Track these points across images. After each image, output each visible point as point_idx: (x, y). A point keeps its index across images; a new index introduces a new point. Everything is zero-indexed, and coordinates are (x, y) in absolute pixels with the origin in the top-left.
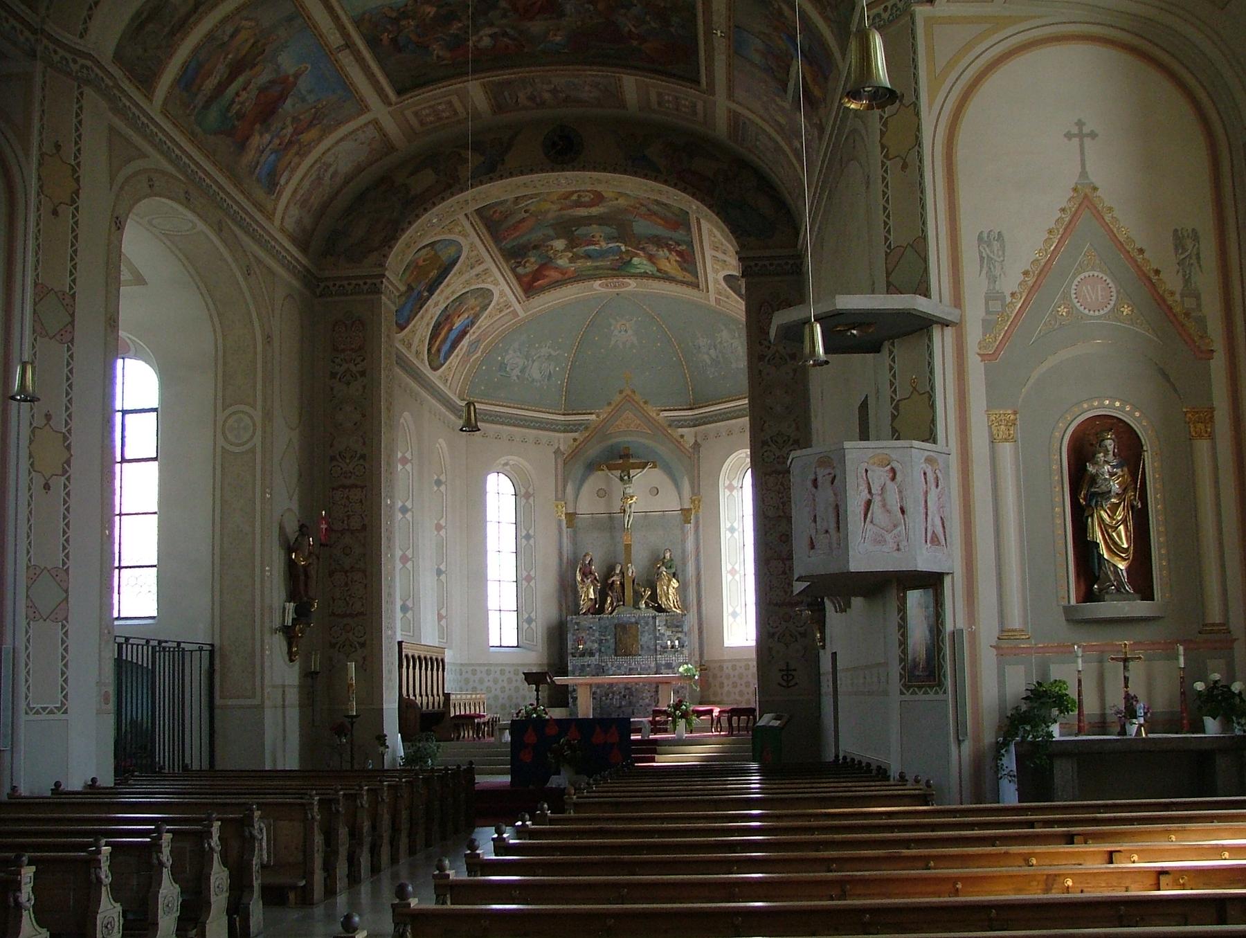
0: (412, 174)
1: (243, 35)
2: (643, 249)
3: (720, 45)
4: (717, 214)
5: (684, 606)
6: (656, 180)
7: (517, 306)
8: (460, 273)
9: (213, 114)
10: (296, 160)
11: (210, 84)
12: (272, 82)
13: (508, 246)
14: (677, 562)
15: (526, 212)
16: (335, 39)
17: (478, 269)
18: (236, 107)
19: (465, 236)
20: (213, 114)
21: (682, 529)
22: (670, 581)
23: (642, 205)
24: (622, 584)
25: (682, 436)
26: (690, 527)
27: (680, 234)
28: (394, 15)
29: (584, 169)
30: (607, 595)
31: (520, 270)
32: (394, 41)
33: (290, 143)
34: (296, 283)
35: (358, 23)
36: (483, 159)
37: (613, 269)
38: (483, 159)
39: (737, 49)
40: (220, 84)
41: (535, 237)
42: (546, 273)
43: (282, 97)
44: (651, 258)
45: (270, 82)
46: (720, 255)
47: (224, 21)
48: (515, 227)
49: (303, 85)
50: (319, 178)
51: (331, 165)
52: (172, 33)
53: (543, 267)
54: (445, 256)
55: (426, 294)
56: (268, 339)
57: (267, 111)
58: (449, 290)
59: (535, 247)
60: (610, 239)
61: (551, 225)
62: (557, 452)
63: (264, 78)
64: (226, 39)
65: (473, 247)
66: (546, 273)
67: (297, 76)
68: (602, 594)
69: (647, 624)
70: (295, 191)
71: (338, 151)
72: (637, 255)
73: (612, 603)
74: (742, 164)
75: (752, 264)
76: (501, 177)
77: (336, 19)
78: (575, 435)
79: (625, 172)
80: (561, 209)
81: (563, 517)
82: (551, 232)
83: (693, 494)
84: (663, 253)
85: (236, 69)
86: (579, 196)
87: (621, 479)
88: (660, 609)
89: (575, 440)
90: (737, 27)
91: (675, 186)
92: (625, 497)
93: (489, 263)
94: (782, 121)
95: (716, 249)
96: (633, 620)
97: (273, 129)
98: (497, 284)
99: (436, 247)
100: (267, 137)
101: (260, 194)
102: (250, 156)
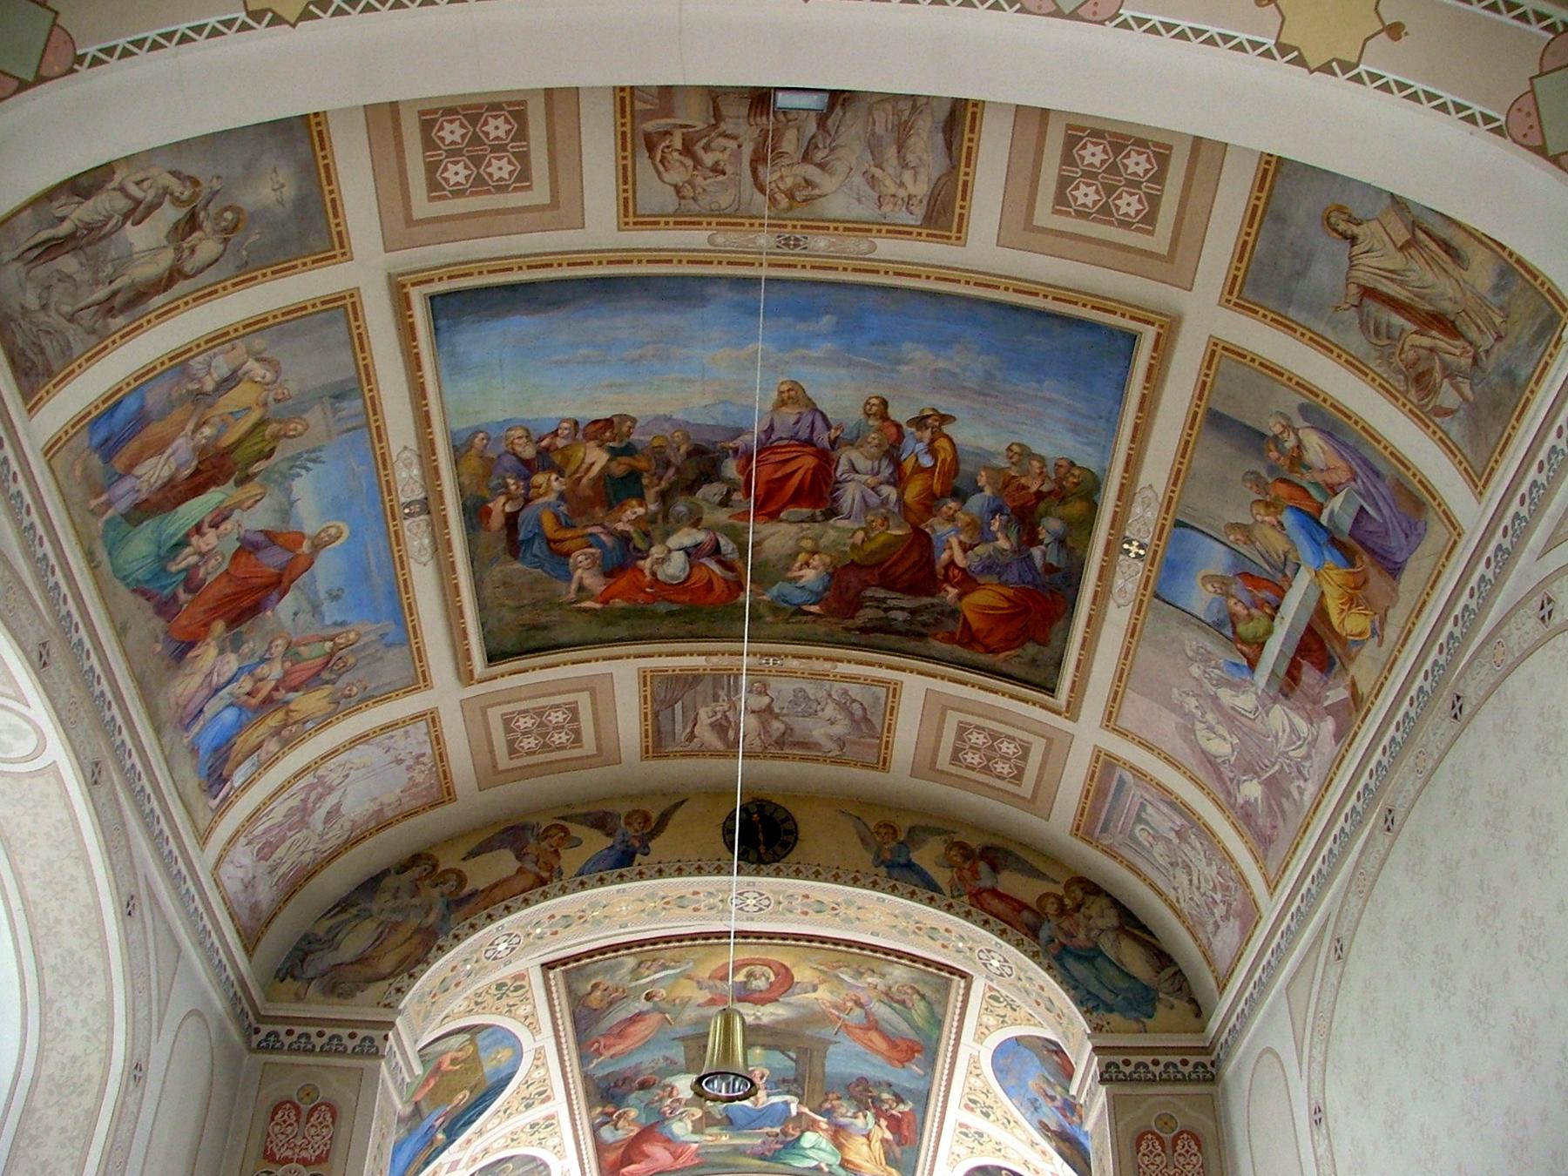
0: (472, 854)
1: (242, 395)
2: (828, 1113)
3: (1129, 578)
4: (1048, 969)
6: (931, 901)
8: (506, 1112)
9: (141, 546)
10: (272, 746)
11: (154, 472)
12: (271, 536)
13: (600, 1073)
15: (649, 997)
16: (407, 481)
17: (538, 1112)
18: (187, 558)
19: (534, 1028)
20: (141, 546)
23: (858, 1003)
27: (904, 1076)
28: (529, 452)
29: (797, 874)
31: (607, 1134)
32: (511, 521)
33: (269, 701)
34: (218, 1003)
35: (459, 452)
36: (609, 842)
37: (762, 1157)
38: (609, 842)
39: (1160, 593)
40: (170, 483)
41: (648, 1060)
42: (647, 1148)
43: (279, 584)
44: (838, 1134)
45: (266, 533)
46: (976, 1121)
47: (219, 339)
48: (621, 1031)
49: (326, 571)
50: (305, 810)
51: (331, 789)
52: (108, 308)
53: (647, 1133)
54: (494, 1060)
55: (440, 1136)
56: (136, 1072)
57: (245, 602)
58: (478, 1145)
59: (644, 1086)
60: (781, 1083)
61: (683, 1039)
63: (257, 519)
64: (209, 386)
65: (539, 1054)
66: (647, 1148)
67: (318, 546)
70: (253, 817)
71: (350, 768)
72: (813, 1126)
74: (1091, 888)
75: (1119, 1059)
76: (641, 876)
77: (423, 420)
79: (874, 885)
82: (678, 1053)
84: (865, 1121)
85: (213, 468)
86: (750, 975)
90: (1179, 524)
91: (967, 915)
93: (559, 1105)
94: (1220, 747)
95: (971, 1104)
97: (245, 649)
98: (561, 1155)
99: (479, 1037)
100: (232, 663)
101: (192, 783)
102: (187, 685)
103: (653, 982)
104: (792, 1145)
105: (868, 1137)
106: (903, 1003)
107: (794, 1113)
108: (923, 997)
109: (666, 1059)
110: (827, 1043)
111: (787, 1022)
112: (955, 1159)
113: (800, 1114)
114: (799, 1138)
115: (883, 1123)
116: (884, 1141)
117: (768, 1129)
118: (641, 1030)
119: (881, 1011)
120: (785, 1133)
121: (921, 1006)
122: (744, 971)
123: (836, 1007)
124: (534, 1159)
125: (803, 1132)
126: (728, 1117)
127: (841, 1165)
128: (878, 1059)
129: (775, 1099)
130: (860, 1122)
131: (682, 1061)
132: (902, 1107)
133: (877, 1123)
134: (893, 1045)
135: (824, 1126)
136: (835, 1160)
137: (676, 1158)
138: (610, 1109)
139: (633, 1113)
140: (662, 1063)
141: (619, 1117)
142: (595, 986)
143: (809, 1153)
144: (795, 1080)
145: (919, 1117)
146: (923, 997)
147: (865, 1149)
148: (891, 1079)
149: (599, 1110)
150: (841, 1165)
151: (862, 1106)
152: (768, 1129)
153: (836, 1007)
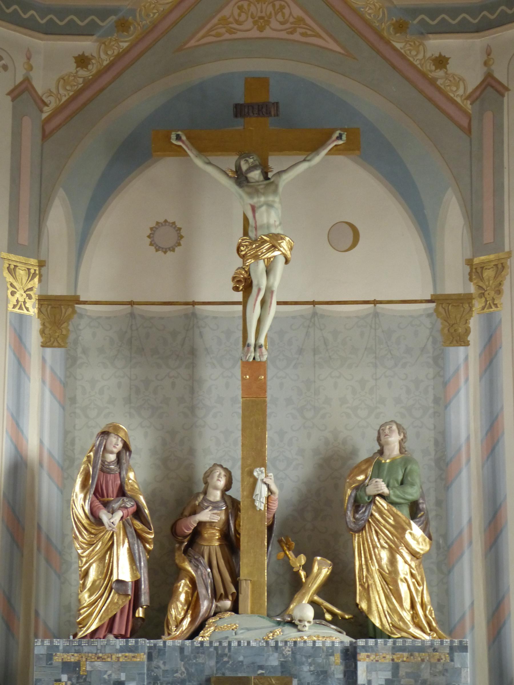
5: (446, 617)
14: (423, 471)
21: (439, 361)
22: (400, 529)
24: (231, 543)
25: (441, 62)
26: (466, 358)
30: (178, 573)
62: (23, 92)
68: (163, 575)
69: (323, 674)
73: (193, 604)
78: (86, 45)
81: (32, 309)
83: (477, 243)
87: (240, 178)
88: (359, 626)
89: (82, 61)
92: (253, 241)
96: (274, 661)
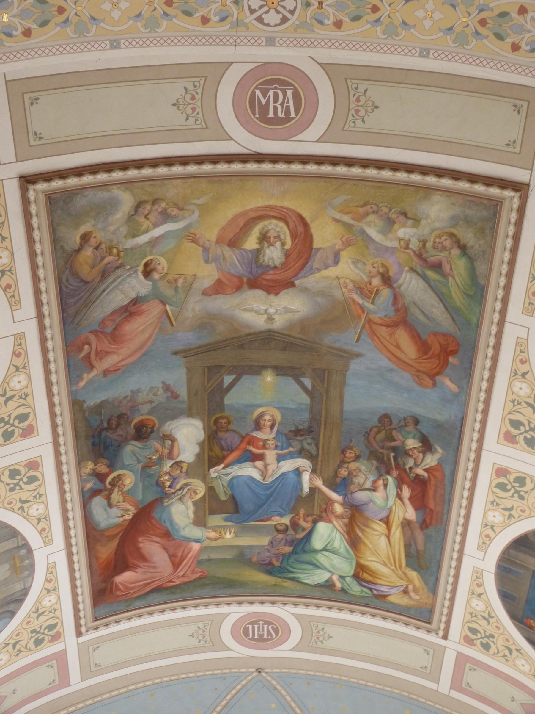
2: (341, 485)
7: (70, 643)
13: (92, 401)
15: (148, 272)
37: (269, 568)
59: (142, 432)
61: (185, 353)
72: (324, 513)
80: (218, 288)
82: (178, 377)
86: (264, 238)
98: (48, 541)
103: (154, 242)
104: (301, 545)
105: (387, 521)
106: (437, 267)
107: (306, 490)
108: (463, 248)
109: (167, 388)
110: (347, 356)
111: (303, 324)
112: (490, 530)
113: (313, 490)
114: (309, 535)
115: (406, 493)
116: (406, 524)
117: (276, 520)
118: (139, 329)
119: (412, 286)
120: (295, 525)
121: (459, 266)
122: (256, 232)
123: (360, 290)
124: (14, 533)
125: (315, 522)
126: (233, 498)
127: (356, 576)
128: (405, 378)
129: (288, 466)
130: (378, 497)
131: (183, 392)
132: (431, 460)
133: (399, 496)
134: (423, 347)
135: (338, 509)
136: (347, 568)
137: (176, 566)
138: (102, 469)
139: (129, 480)
140: (161, 397)
141: (113, 484)
142: (85, 238)
143: (321, 558)
144: (309, 431)
145: (447, 472)
146: (463, 248)
147: (383, 540)
148: (419, 411)
149: (90, 466)
150: (356, 576)
151: (384, 467)
152: (276, 520)
153: (360, 290)
